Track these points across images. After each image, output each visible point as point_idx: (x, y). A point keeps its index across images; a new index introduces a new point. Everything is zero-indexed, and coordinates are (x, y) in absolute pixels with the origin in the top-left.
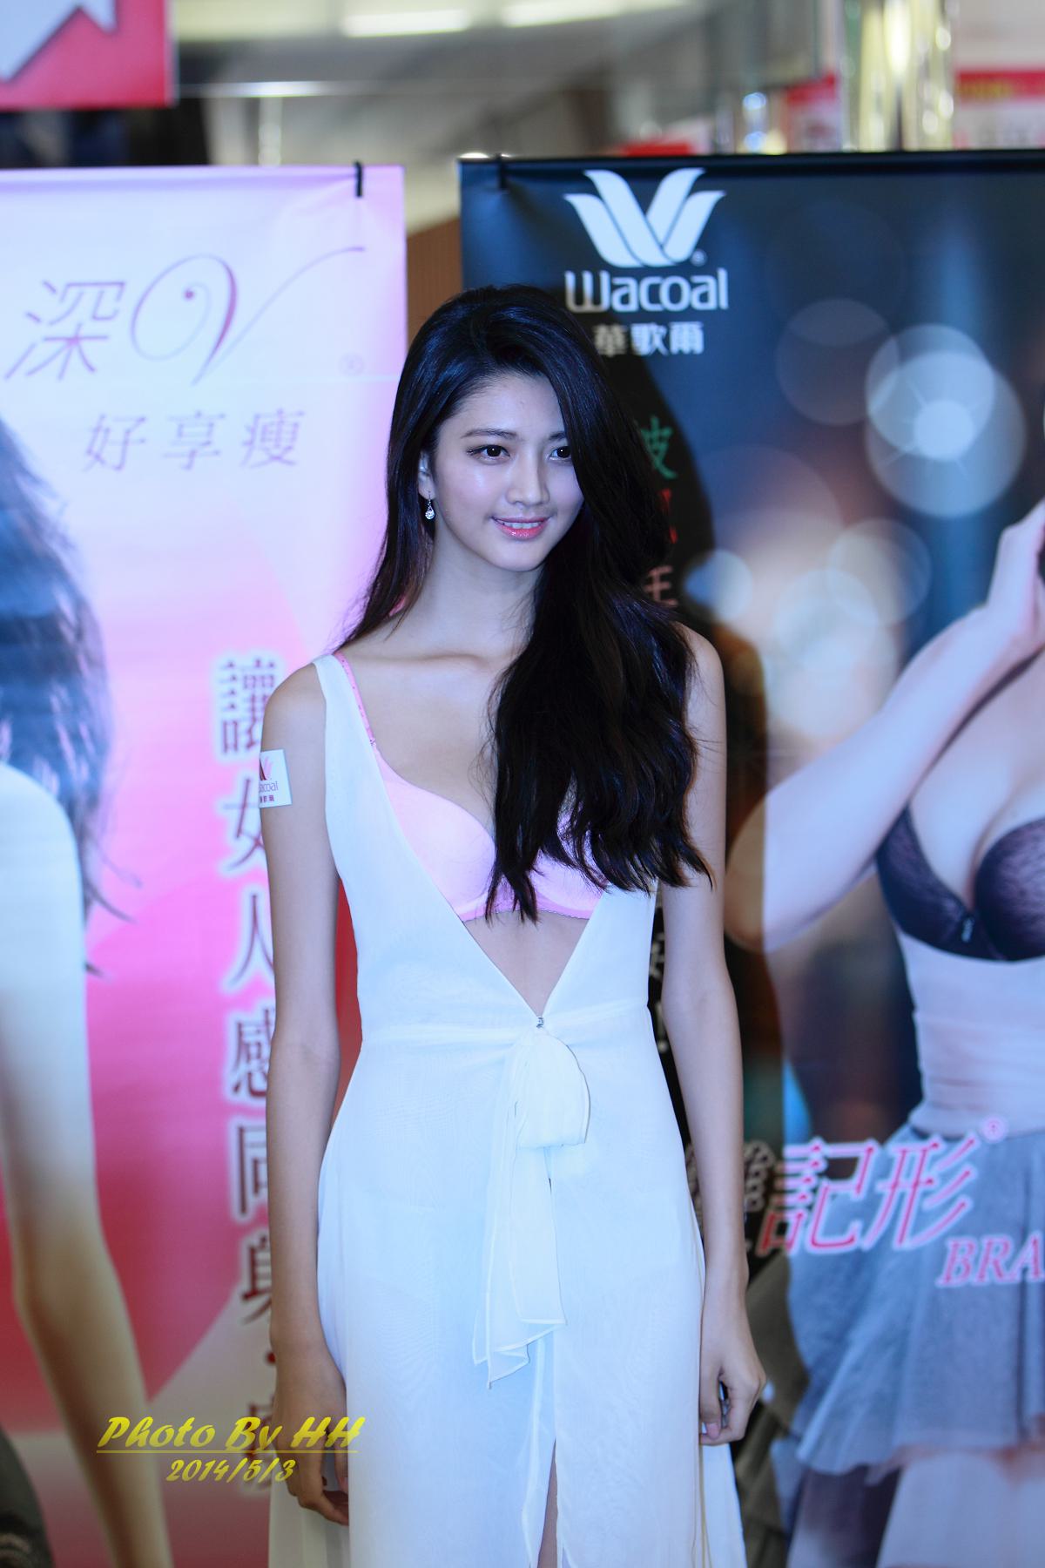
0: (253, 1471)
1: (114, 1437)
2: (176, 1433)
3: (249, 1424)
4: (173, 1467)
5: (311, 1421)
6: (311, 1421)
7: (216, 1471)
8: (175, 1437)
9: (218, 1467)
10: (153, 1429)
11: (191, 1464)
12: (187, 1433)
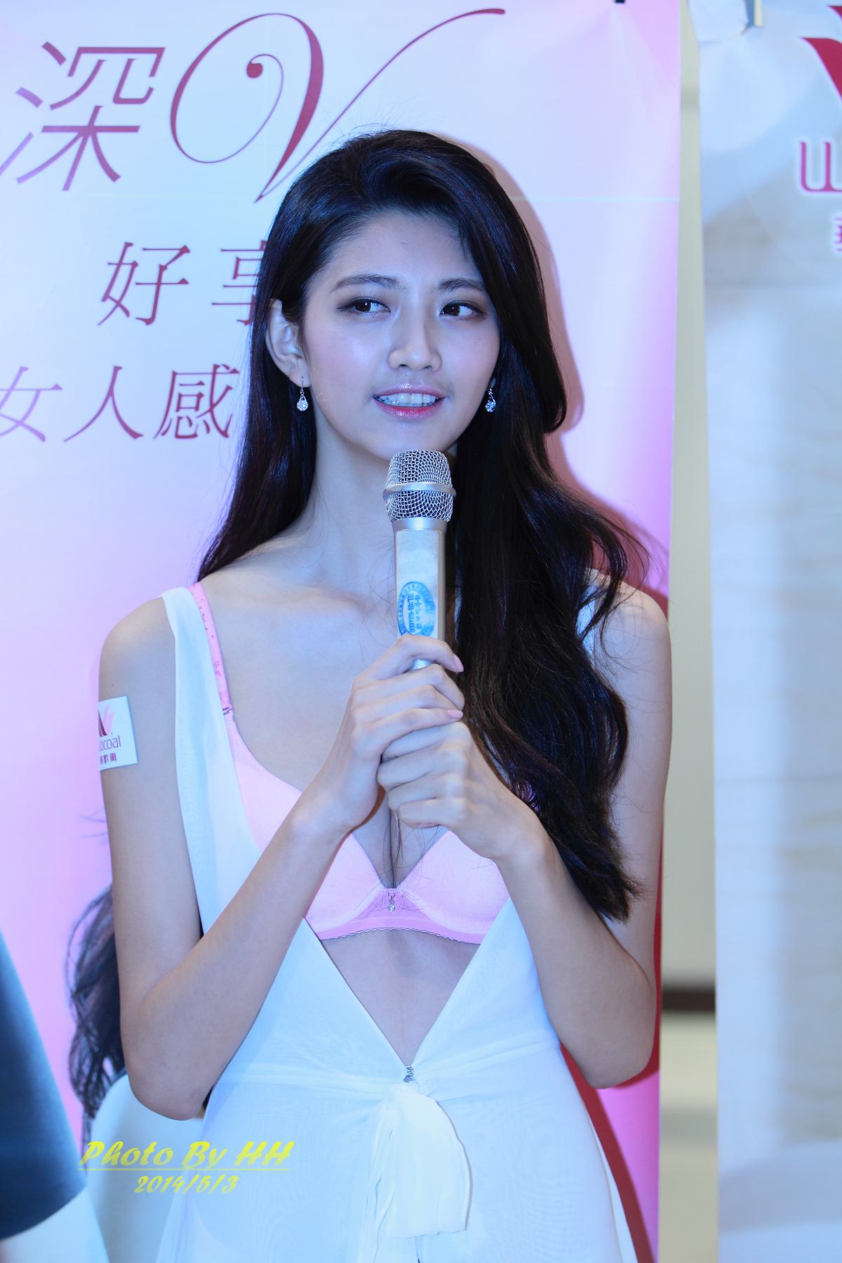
0: (204, 1184)
1: (92, 1157)
2: (142, 1154)
3: (200, 1147)
4: (139, 1182)
5: (251, 1144)
6: (251, 1144)
7: (174, 1185)
8: (141, 1157)
9: (176, 1181)
10: (123, 1151)
11: (154, 1179)
12: (151, 1154)
